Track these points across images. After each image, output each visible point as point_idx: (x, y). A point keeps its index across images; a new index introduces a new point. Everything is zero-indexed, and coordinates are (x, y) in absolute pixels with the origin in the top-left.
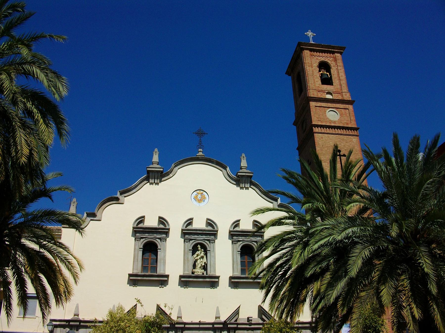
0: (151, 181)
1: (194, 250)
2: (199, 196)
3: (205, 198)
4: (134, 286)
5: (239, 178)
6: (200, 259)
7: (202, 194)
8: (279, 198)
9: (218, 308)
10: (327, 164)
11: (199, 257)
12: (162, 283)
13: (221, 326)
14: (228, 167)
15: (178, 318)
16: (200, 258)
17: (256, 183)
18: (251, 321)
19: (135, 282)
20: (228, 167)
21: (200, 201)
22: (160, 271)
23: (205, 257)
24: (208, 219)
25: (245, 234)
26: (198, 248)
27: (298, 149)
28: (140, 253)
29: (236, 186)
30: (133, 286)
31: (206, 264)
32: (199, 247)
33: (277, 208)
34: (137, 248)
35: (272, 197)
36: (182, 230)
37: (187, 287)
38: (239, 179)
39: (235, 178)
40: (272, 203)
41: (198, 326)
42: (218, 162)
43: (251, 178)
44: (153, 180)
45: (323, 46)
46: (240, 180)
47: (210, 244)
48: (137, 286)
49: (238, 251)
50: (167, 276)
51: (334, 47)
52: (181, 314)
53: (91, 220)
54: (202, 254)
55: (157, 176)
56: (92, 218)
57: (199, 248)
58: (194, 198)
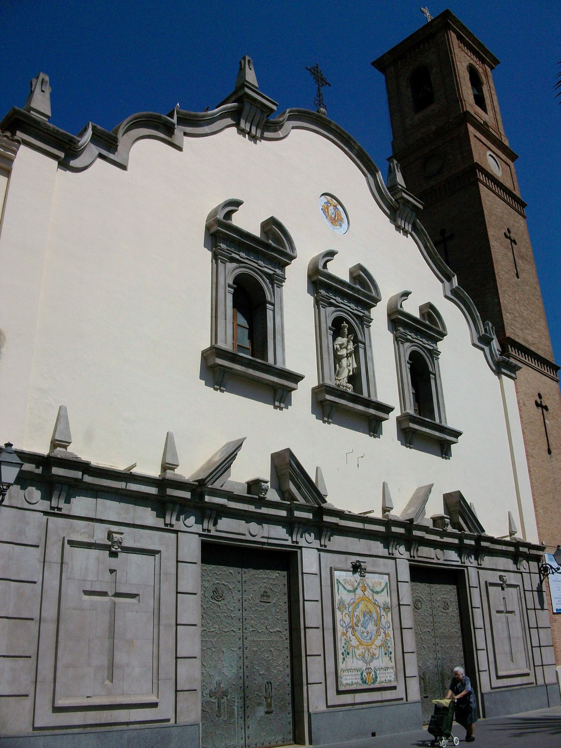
0: (243, 124)
3: (342, 220)
4: (218, 387)
5: (399, 203)
7: (336, 206)
8: (456, 276)
14: (380, 172)
17: (422, 230)
20: (380, 172)
24: (360, 267)
29: (388, 219)
30: (216, 386)
32: (345, 327)
37: (330, 420)
38: (398, 206)
39: (391, 200)
40: (442, 281)
41: (359, 525)
42: (364, 153)
44: (248, 125)
45: (475, 40)
46: (398, 209)
48: (224, 389)
51: (486, 52)
54: (351, 346)
55: (260, 118)
56: (105, 153)
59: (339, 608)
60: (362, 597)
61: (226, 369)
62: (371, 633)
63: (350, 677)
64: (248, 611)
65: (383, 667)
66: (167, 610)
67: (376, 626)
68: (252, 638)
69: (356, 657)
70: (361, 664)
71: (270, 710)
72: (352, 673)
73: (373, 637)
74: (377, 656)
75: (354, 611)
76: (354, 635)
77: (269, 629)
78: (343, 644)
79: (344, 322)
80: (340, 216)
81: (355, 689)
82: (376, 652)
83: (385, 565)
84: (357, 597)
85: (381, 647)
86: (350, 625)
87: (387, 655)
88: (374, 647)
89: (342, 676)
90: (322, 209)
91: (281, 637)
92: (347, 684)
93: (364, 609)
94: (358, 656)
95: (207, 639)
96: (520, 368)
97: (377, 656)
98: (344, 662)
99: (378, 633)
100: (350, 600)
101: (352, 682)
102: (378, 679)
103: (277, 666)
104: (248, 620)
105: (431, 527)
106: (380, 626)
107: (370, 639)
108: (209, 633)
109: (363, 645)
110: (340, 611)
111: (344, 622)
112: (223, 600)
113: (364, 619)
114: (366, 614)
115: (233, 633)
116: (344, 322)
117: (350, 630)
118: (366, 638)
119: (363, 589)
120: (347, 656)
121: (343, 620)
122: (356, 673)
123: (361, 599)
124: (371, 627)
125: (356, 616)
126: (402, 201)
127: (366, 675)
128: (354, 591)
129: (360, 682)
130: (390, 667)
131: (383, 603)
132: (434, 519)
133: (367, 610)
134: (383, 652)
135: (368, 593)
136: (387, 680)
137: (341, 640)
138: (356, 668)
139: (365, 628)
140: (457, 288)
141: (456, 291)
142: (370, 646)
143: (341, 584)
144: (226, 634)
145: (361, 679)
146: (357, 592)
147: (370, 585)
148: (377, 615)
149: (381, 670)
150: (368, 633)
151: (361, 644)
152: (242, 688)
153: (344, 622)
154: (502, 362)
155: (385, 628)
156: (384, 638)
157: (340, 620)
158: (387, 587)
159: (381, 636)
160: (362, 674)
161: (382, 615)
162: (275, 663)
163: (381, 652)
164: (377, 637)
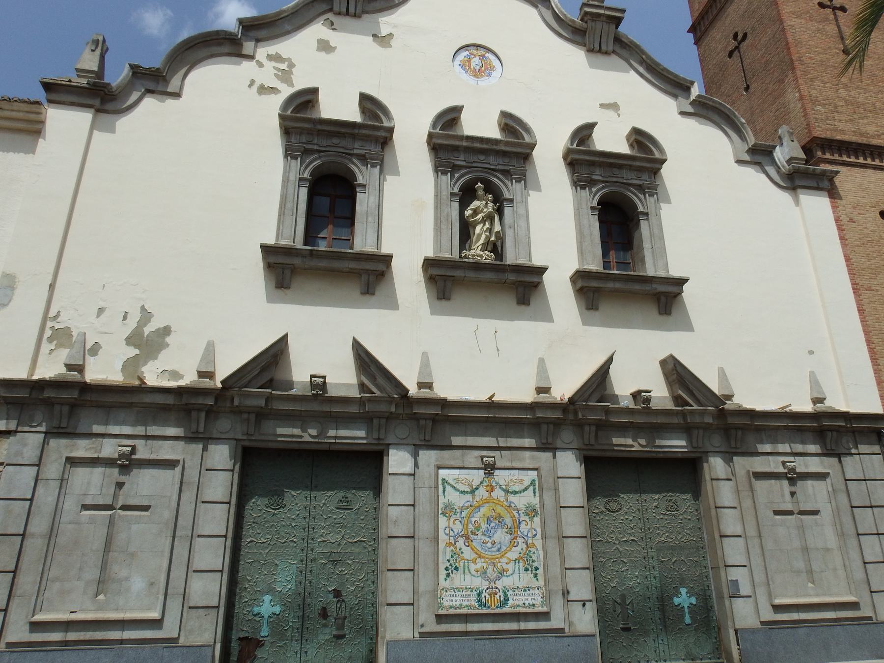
1: (466, 195)
2: (476, 62)
3: (492, 68)
5: (586, 22)
6: (483, 221)
7: (483, 56)
9: (541, 361)
10: (803, 22)
11: (480, 216)
12: (369, 279)
13: (558, 415)
15: (421, 385)
16: (483, 218)
18: (648, 400)
19: (283, 273)
21: (477, 74)
22: (363, 242)
23: (497, 218)
25: (610, 161)
26: (475, 191)
27: (693, 29)
28: (304, 192)
31: (500, 237)
33: (690, 109)
34: (294, 177)
35: (675, 79)
36: (431, 136)
43: (617, 27)
47: (512, 184)
49: (592, 208)
50: (387, 259)
52: (430, 375)
57: (481, 193)
58: (460, 65)
59: (444, 514)
60: (486, 499)
61: (284, 265)
62: (500, 543)
63: (458, 598)
64: (317, 519)
65: (520, 586)
66: (185, 521)
67: (510, 534)
68: (321, 549)
69: (470, 572)
70: (479, 583)
71: (341, 633)
72: (461, 593)
73: (504, 548)
74: (510, 572)
75: (470, 516)
76: (468, 546)
77: (347, 538)
78: (448, 557)
79: (479, 183)
80: (490, 64)
81: (466, 613)
82: (510, 567)
83: (533, 458)
84: (478, 499)
85: (517, 561)
86: (462, 533)
87: (529, 572)
88: (504, 560)
89: (443, 596)
90: (460, 65)
91: (365, 548)
92: (451, 607)
93: (489, 514)
94: (473, 572)
95: (255, 551)
96: (838, 172)
97: (510, 572)
98: (448, 579)
99: (513, 543)
100: (465, 503)
101: (461, 605)
102: (510, 602)
103: (355, 581)
104: (317, 529)
105: (632, 406)
106: (517, 534)
107: (499, 551)
108: (259, 544)
109: (484, 558)
110: (447, 517)
111: (452, 530)
112: (282, 508)
113: (488, 526)
114: (492, 519)
115: (292, 544)
116: (479, 183)
117: (461, 541)
118: (490, 550)
119: (490, 489)
120: (455, 571)
121: (449, 527)
122: (469, 593)
123: (485, 501)
124: (500, 535)
125: (473, 522)
126: (590, 18)
127: (488, 596)
128: (473, 492)
130: (535, 586)
131: (525, 505)
132: (635, 395)
133: (494, 514)
134: (521, 567)
135: (498, 493)
136: (527, 604)
137: (445, 552)
138: (468, 587)
139: (490, 537)
140: (699, 96)
141: (700, 102)
142: (497, 560)
143: (449, 484)
144: (282, 545)
145: (478, 602)
146: (477, 493)
147: (502, 483)
148: (513, 520)
149: (516, 591)
150: (495, 543)
151: (480, 557)
152: (301, 606)
153: (452, 530)
154: (794, 172)
155: (527, 536)
156: (525, 550)
157: (444, 527)
158: (534, 486)
159: (519, 548)
160: (479, 595)
161: (521, 520)
162: (353, 577)
163: (517, 567)
164: (511, 549)
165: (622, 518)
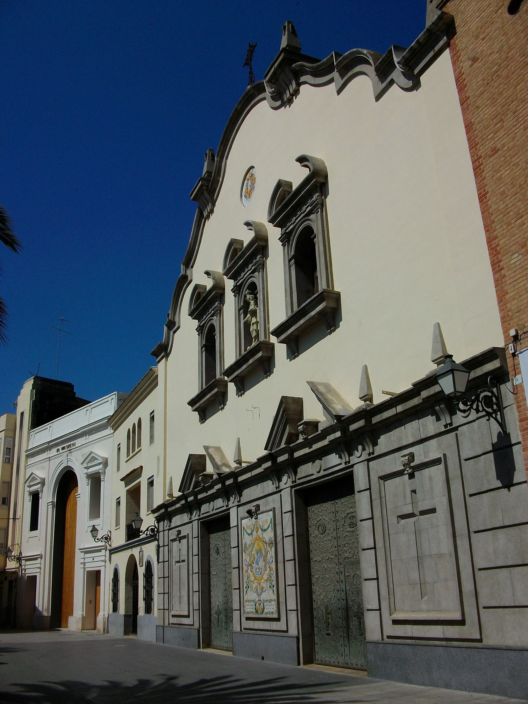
53: (175, 332)
82: (264, 585)
88: (263, 581)
102: (265, 610)
124: (261, 563)
127: (258, 606)
129: (254, 611)
139: (258, 565)
143: (245, 530)
147: (261, 524)
155: (270, 562)
165: (326, 539)
